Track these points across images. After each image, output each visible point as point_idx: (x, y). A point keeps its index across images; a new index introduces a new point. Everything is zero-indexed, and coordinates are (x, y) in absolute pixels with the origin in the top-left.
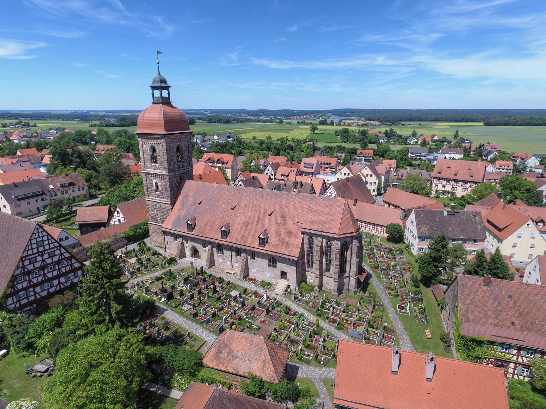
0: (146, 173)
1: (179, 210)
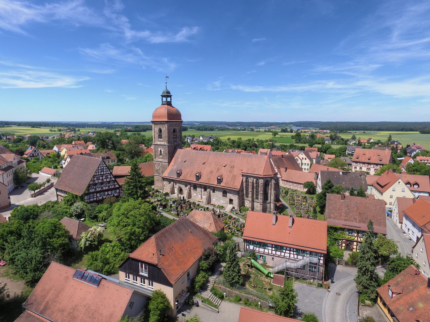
0: (155, 145)
1: (172, 166)
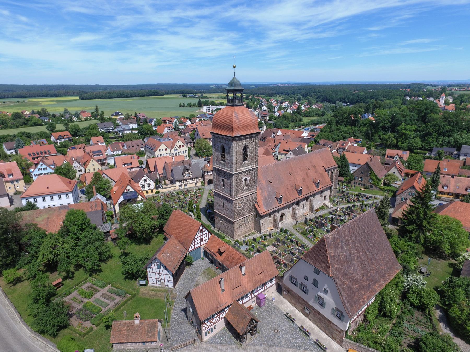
0: (237, 174)
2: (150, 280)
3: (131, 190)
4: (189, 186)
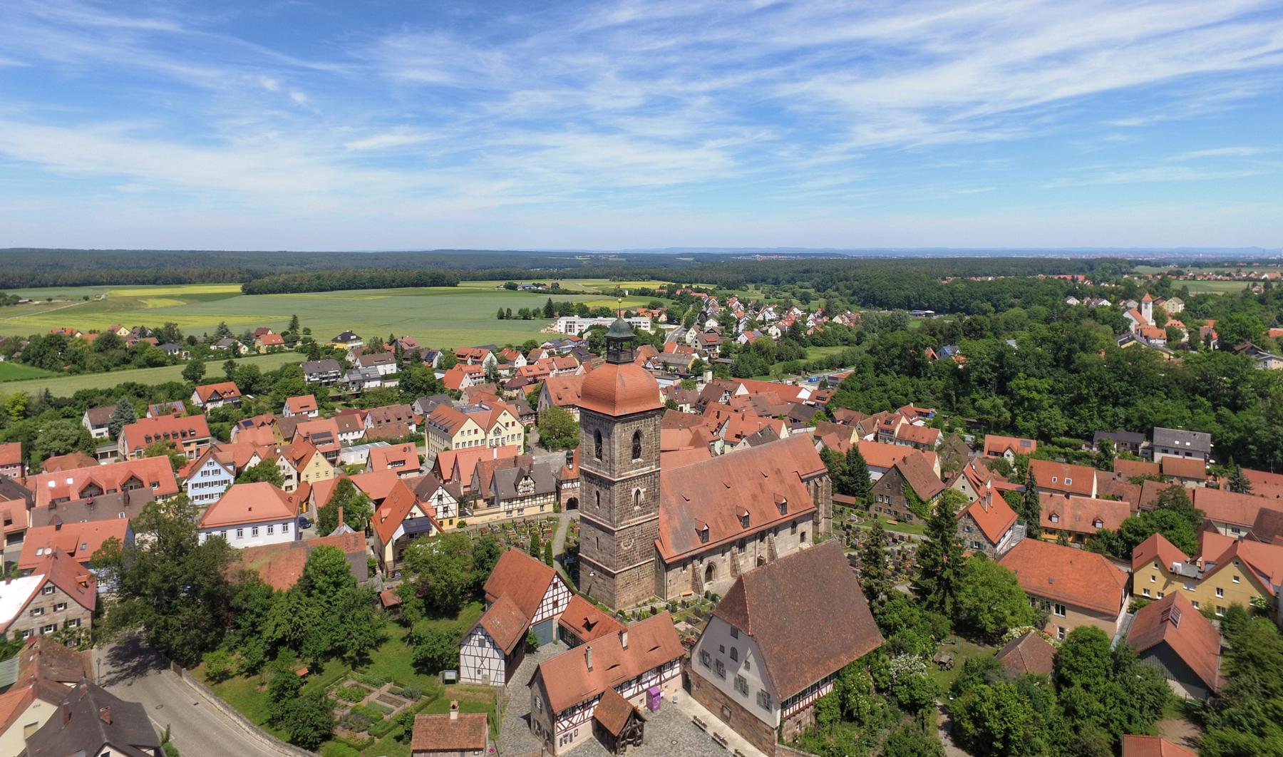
1: (668, 521)
2: (463, 671)
3: (420, 514)
4: (527, 512)
